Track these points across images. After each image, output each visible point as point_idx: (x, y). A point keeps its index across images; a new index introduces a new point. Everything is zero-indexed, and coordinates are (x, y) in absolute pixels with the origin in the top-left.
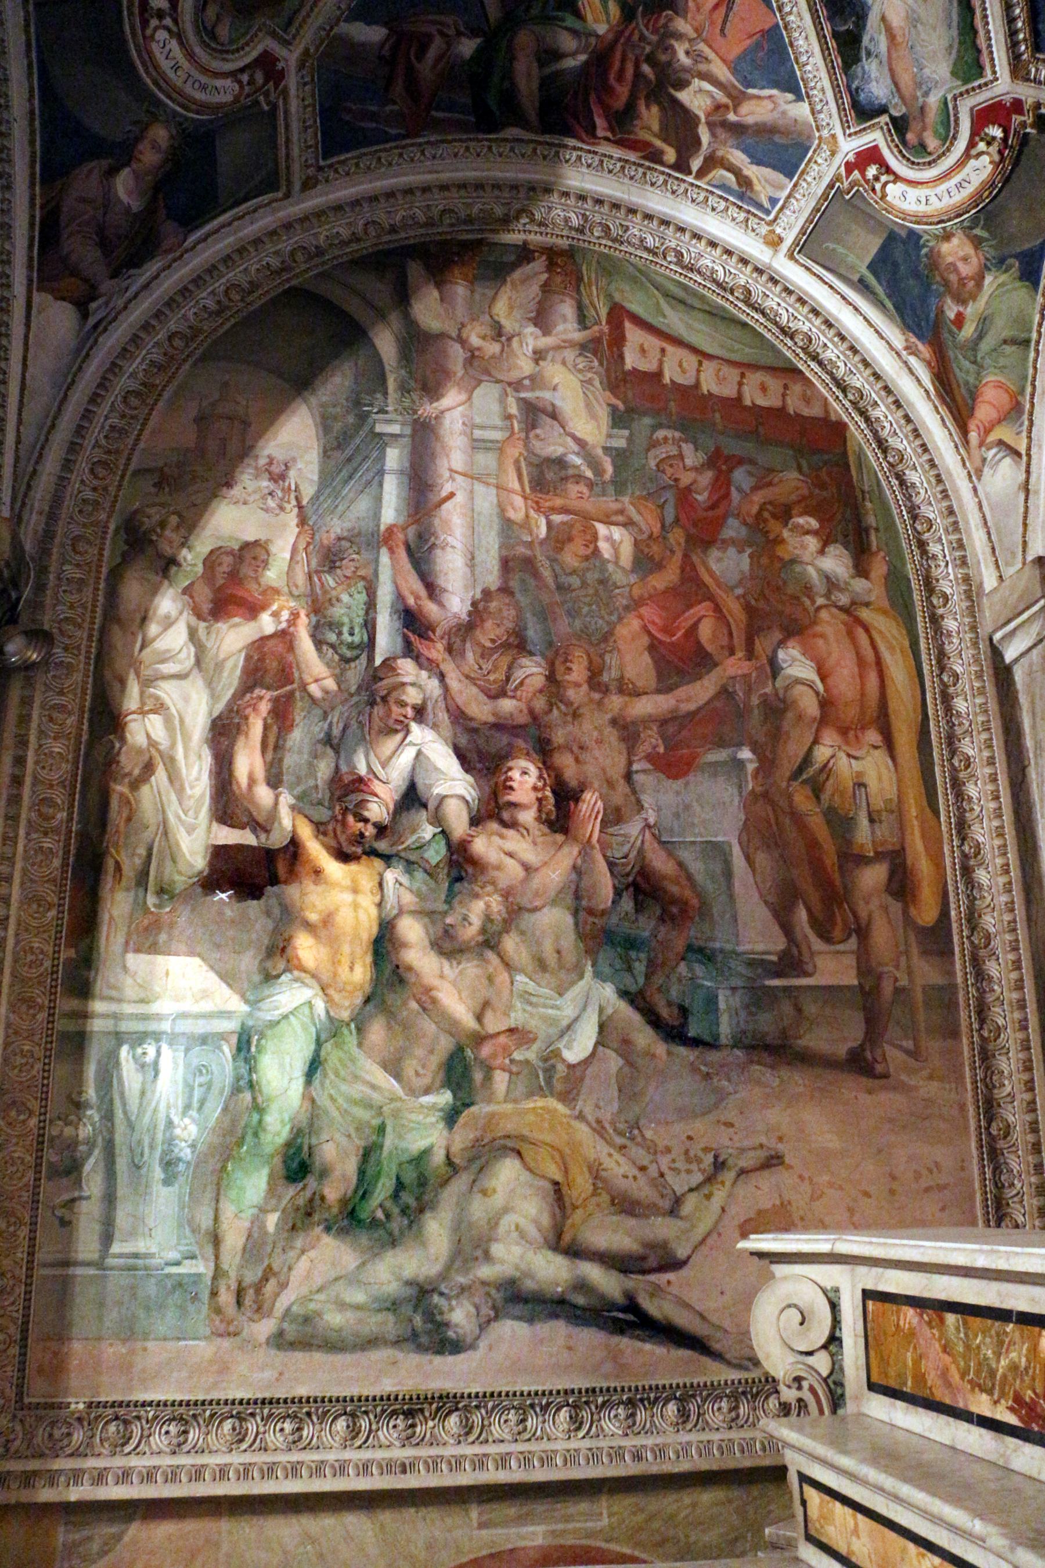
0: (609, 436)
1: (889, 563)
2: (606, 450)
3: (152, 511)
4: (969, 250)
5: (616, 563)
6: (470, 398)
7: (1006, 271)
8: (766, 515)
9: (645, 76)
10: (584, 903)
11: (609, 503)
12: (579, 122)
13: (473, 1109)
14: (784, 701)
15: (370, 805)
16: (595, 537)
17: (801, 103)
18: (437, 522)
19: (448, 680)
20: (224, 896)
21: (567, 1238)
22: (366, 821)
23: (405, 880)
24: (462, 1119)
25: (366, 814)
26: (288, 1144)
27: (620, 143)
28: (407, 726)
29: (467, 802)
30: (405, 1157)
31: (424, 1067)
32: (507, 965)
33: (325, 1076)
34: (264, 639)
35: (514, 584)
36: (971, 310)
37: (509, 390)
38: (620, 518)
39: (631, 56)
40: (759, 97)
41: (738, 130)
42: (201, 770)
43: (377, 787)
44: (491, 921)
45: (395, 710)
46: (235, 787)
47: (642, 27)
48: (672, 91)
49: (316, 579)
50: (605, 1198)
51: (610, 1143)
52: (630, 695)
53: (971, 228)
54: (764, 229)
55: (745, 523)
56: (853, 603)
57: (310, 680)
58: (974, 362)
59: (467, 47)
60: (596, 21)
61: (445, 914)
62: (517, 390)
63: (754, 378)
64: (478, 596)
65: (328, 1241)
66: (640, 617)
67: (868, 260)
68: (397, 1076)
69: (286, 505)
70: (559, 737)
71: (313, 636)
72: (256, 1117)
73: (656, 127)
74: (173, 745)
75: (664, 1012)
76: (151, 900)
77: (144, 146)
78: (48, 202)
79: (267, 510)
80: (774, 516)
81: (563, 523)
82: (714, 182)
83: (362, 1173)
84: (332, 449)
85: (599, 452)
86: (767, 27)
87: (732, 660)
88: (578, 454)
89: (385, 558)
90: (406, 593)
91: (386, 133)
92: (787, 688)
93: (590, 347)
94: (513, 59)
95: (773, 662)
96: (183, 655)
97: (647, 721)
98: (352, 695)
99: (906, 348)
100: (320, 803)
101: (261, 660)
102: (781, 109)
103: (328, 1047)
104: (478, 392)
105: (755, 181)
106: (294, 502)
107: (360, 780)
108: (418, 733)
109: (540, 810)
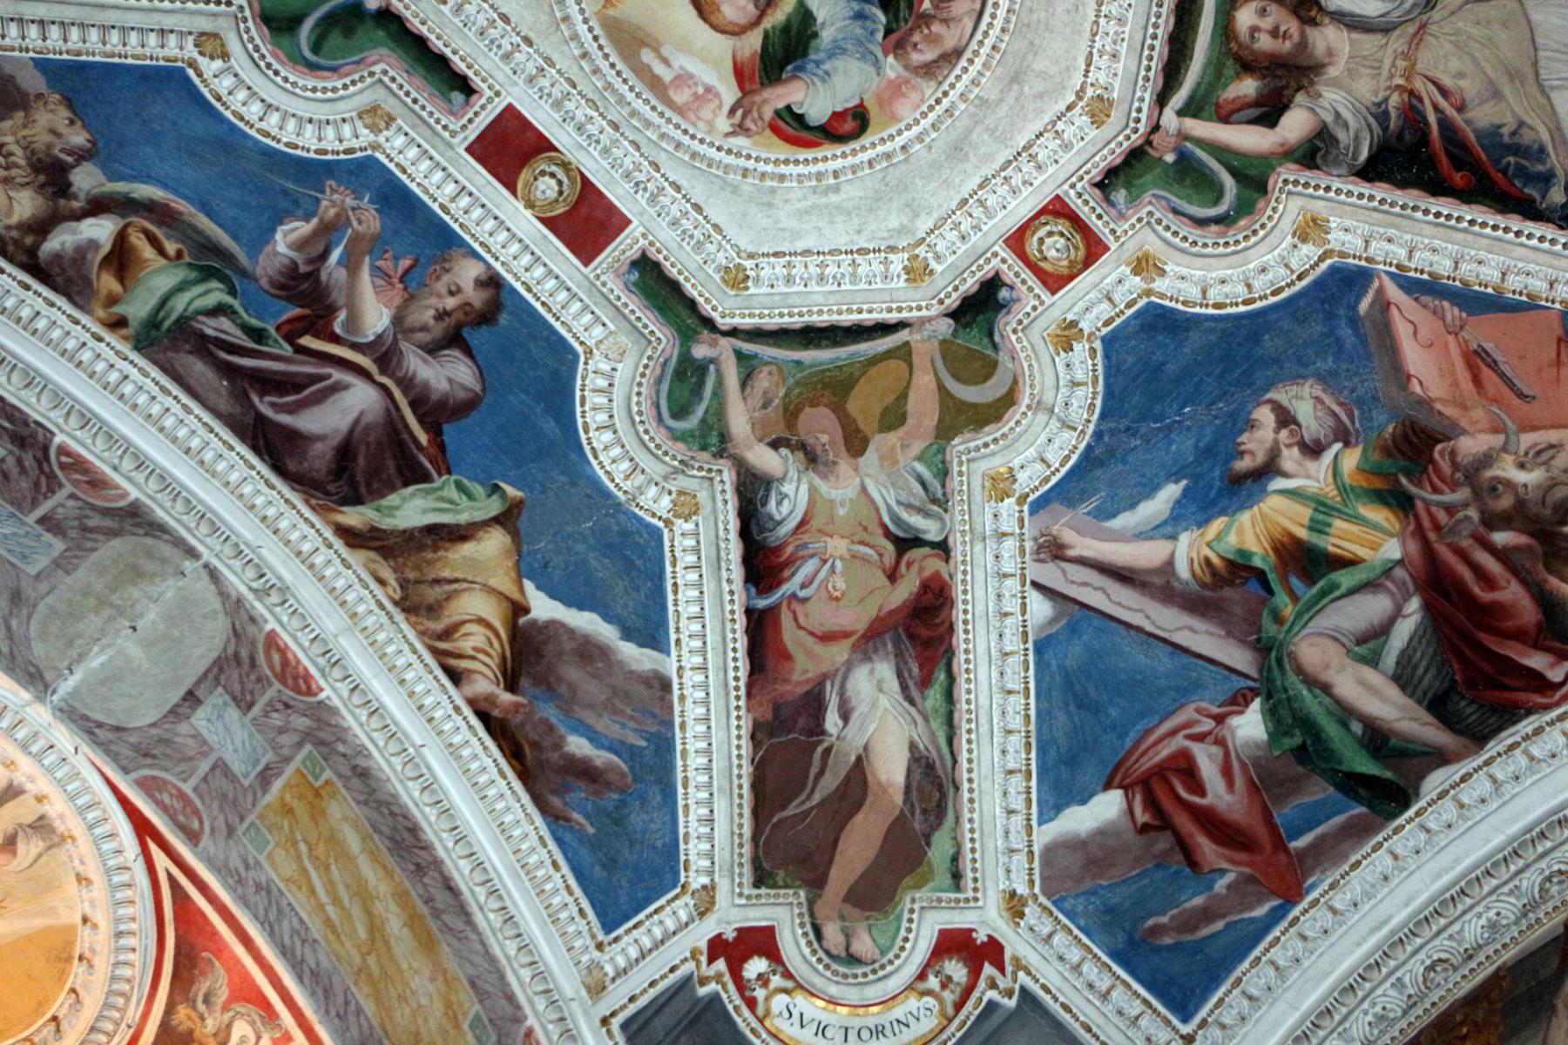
9: (1517, 548)
39: (1465, 543)
59: (1250, 726)
60: (1375, 547)
91: (1252, 920)
94: (1326, 688)
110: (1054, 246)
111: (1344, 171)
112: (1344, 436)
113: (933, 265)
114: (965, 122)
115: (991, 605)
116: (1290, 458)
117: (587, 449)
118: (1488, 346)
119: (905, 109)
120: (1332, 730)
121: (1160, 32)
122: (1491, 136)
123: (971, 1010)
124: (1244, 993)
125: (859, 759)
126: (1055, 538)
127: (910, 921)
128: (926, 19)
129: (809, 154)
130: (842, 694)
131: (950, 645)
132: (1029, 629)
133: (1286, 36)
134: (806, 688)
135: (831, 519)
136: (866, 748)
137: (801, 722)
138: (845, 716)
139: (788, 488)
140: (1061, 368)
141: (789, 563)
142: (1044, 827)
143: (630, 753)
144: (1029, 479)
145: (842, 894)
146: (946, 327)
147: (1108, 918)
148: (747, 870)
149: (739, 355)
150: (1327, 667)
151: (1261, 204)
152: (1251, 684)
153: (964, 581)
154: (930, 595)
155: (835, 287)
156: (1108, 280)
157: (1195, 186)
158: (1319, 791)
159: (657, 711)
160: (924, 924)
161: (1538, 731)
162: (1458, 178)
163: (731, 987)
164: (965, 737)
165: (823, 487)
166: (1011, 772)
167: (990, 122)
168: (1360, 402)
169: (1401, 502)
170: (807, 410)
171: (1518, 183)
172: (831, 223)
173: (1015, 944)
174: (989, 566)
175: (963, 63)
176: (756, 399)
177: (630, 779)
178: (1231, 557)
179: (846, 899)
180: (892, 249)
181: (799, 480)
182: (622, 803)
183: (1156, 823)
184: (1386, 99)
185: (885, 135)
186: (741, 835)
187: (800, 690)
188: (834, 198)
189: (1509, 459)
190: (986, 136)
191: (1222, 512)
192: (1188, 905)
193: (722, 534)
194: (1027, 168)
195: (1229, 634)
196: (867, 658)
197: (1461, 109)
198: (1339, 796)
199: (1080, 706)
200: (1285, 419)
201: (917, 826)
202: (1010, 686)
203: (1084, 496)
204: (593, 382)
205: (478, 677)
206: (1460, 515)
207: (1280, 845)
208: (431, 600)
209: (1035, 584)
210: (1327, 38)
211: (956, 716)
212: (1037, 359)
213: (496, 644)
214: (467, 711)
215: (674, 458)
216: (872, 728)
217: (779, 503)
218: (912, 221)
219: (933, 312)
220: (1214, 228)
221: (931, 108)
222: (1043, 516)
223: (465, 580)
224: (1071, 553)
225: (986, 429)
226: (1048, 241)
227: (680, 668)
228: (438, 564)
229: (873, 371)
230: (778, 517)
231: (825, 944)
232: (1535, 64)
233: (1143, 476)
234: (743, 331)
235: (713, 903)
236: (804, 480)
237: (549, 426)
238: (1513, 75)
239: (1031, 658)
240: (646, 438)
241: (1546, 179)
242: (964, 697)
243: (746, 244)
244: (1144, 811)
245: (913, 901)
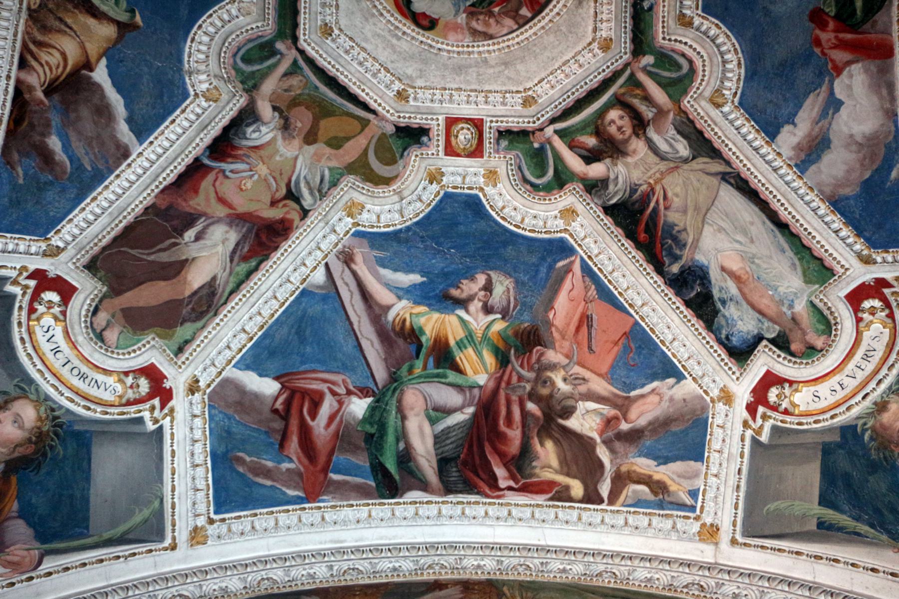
12: (478, 476)
27: (525, 489)
39: (514, 398)
40: (642, 396)
41: (633, 437)
47: (519, 369)
48: (561, 421)
54: (696, 527)
59: (359, 407)
60: (476, 372)
73: (555, 462)
82: (630, 501)
86: (627, 329)
91: (284, 494)
94: (404, 418)
102: (666, 398)
105: (669, 482)
110: (464, 136)
111: (599, 203)
112: (505, 314)
113: (411, 99)
114: (472, 62)
115: (304, 253)
116: (476, 306)
117: (191, 35)
119: (452, 37)
120: (390, 438)
121: (577, 94)
122: (669, 227)
123: (132, 412)
124: (253, 522)
125: (187, 260)
126: (353, 254)
127: (144, 346)
128: (491, 14)
129: (400, 17)
130: (205, 228)
131: (270, 254)
132: (308, 280)
133: (623, 133)
134: (192, 211)
135: (271, 157)
136: (194, 259)
137: (175, 222)
138: (198, 238)
139: (264, 129)
140: (421, 187)
141: (236, 157)
142: (234, 369)
143: (78, 167)
144: (366, 218)
145: (124, 306)
146: (390, 129)
147: (224, 435)
148: (88, 257)
149: (295, 62)
150: (412, 409)
151: (555, 192)
152: (375, 389)
153: (301, 234)
154: (281, 226)
155: (363, 71)
156: (472, 169)
157: (536, 164)
158: (362, 461)
159: (111, 162)
160: (149, 352)
161: (477, 503)
162: (642, 236)
163: (28, 297)
164: (240, 296)
165: (280, 141)
166: (244, 331)
167: (482, 70)
168: (524, 304)
169: (503, 361)
170: (303, 108)
171: (664, 253)
172: (384, 49)
173: (179, 402)
174: (318, 236)
175: (490, 42)
176: (285, 86)
177: (67, 176)
178: (415, 327)
179: (123, 310)
180: (400, 80)
181: (272, 130)
182: (51, 183)
183: (283, 414)
184: (641, 185)
185: (436, 39)
186: (100, 240)
187: (188, 209)
188: (394, 41)
190: (475, 74)
191: (429, 305)
192: (263, 462)
193: (217, 120)
194: (481, 99)
195: (386, 360)
196: (230, 225)
197: (666, 208)
198: (369, 469)
199: (297, 333)
200: (488, 287)
201: (184, 311)
202: (278, 295)
203: (380, 248)
204: (222, 13)
205: (35, 75)
206: (522, 384)
207: (325, 470)
208: (49, 24)
209: (327, 265)
210: (638, 146)
211: (244, 285)
212: (416, 174)
213: (60, 70)
214: (12, 82)
215: (227, 73)
216: (204, 254)
217: (254, 131)
218: (417, 77)
219: (392, 118)
220: (528, 187)
221: (463, 46)
222: (356, 240)
223: (75, 32)
224: (353, 266)
225: (368, 184)
226: (465, 131)
227: (141, 154)
228: (70, 14)
229: (345, 118)
230: (248, 136)
231: (94, 319)
232: (708, 210)
233: (411, 262)
234: (306, 55)
235: (57, 256)
236: (275, 132)
237: (184, 12)
238: (697, 209)
239: (297, 293)
240: (223, 55)
241: (676, 258)
242: (255, 280)
243: (343, 22)
244: (282, 404)
245: (154, 339)
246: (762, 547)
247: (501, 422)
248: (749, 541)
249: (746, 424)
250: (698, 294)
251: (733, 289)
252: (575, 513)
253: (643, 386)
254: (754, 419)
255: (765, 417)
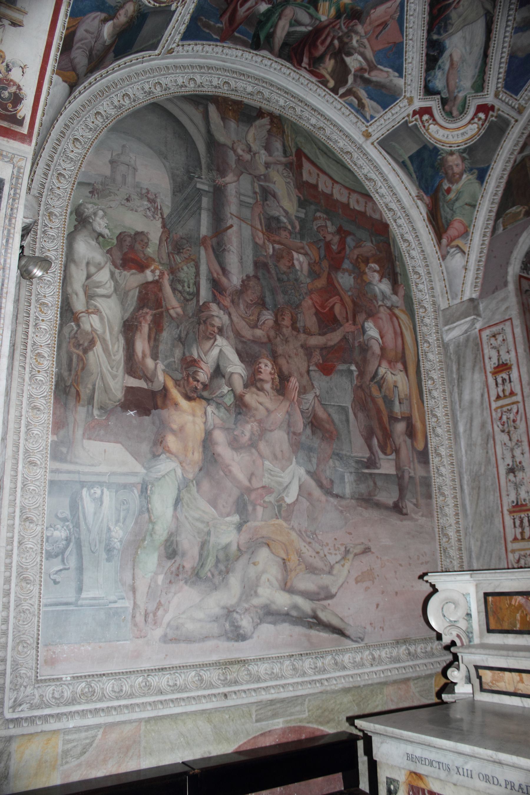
0: (298, 211)
1: (405, 290)
2: (296, 216)
3: (89, 206)
4: (459, 162)
5: (302, 271)
6: (238, 180)
7: (472, 174)
8: (360, 260)
9: (334, 46)
10: (292, 429)
11: (298, 242)
13: (249, 524)
14: (367, 346)
15: (200, 374)
16: (292, 259)
17: (400, 79)
18: (225, 238)
19: (232, 317)
20: (132, 413)
21: (289, 584)
22: (198, 381)
23: (216, 411)
24: (244, 528)
25: (198, 378)
26: (166, 541)
28: (215, 337)
29: (242, 377)
30: (219, 547)
31: (226, 503)
32: (261, 456)
33: (183, 506)
34: (148, 283)
35: (260, 274)
36: (454, 187)
37: (255, 180)
38: (302, 251)
39: (332, 34)
40: (382, 70)
41: (367, 82)
42: (119, 347)
43: (203, 365)
44: (254, 434)
45: (210, 328)
46: (136, 357)
48: (344, 56)
49: (171, 257)
50: (303, 566)
51: (304, 541)
52: (308, 334)
53: (462, 153)
54: (364, 129)
55: (351, 263)
56: (392, 306)
57: (170, 308)
58: (452, 210)
59: (263, 7)
60: (323, 14)
61: (234, 430)
62: (258, 180)
63: (354, 197)
64: (245, 278)
65: (186, 588)
66: (311, 299)
67: (410, 154)
68: (215, 507)
69: (156, 216)
70: (280, 350)
71: (171, 285)
72: (151, 526)
73: (330, 69)
74: (104, 332)
75: (325, 482)
76: (96, 412)
77: (122, 12)
78: (71, 27)
79: (146, 216)
80: (363, 262)
81: (279, 249)
82: (347, 101)
83: (201, 555)
84: (177, 192)
85: (294, 218)
86: (397, 42)
87: (347, 325)
88: (285, 217)
89: (203, 252)
90: (213, 271)
91: (212, 37)
92: (368, 340)
93: (289, 166)
94: (280, 18)
95: (363, 327)
96: (108, 285)
97: (316, 347)
98: (190, 318)
99: (417, 196)
100: (176, 370)
101: (147, 294)
102: (390, 78)
103: (183, 491)
104: (242, 177)
105: (366, 106)
106: (160, 216)
107: (194, 361)
108: (220, 341)
109: (273, 384)
118: (389, 26)
120: (269, 25)
122: (448, 18)
161: (289, 68)
162: (435, 11)
169: (338, 15)
189: (358, 38)
207: (233, 31)
241: (439, 33)
246: (380, 153)
247: (319, 41)
248: (378, 147)
249: (408, 116)
250: (433, 56)
251: (447, 67)
252: (324, 93)
253: (385, 67)
254: (413, 117)
255: (416, 120)
